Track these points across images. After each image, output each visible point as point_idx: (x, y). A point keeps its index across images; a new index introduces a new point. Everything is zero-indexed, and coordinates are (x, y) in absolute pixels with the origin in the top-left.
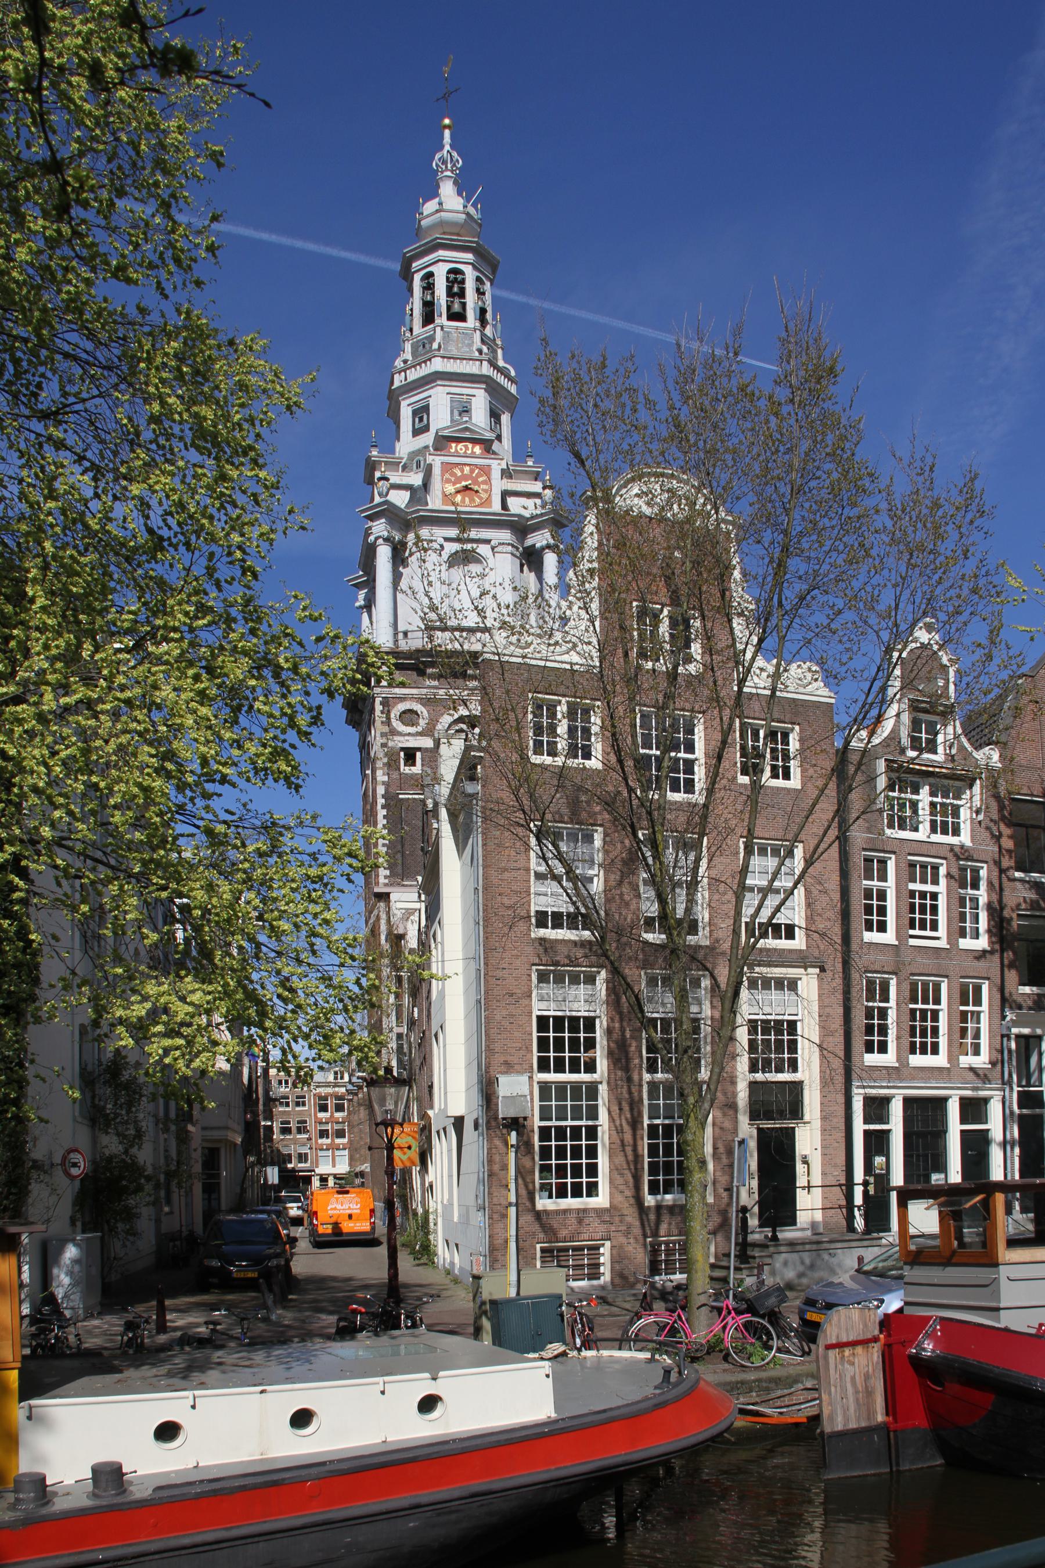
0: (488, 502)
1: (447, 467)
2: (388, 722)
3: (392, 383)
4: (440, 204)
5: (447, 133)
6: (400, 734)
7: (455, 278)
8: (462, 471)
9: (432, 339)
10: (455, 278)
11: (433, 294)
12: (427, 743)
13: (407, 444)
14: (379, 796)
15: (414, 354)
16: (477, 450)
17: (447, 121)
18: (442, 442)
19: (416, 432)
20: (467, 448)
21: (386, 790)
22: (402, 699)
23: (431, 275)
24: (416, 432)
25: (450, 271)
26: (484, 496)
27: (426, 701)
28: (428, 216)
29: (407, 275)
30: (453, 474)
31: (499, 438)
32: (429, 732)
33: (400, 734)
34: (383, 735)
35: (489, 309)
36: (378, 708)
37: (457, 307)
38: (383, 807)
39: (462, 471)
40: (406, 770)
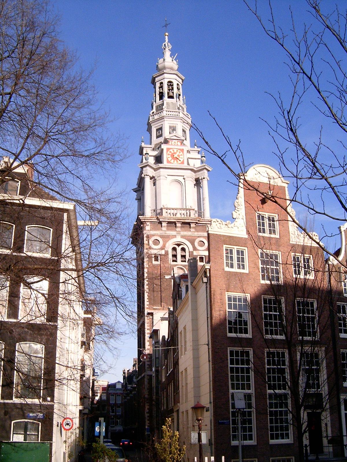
0: (183, 163)
1: (168, 149)
2: (148, 244)
3: (149, 120)
4: (164, 60)
5: (167, 37)
6: (153, 249)
7: (170, 84)
8: (174, 151)
9: (163, 104)
10: (170, 84)
11: (163, 90)
12: (163, 252)
13: (155, 141)
14: (145, 273)
15: (157, 110)
16: (179, 144)
17: (167, 34)
18: (166, 141)
19: (158, 137)
20: (175, 143)
21: (148, 271)
22: (153, 235)
23: (161, 83)
24: (158, 137)
25: (168, 82)
26: (182, 160)
27: (161, 237)
28: (160, 64)
29: (153, 82)
30: (170, 152)
31: (186, 139)
32: (162, 248)
33: (153, 249)
34: (147, 249)
35: (181, 95)
36: (145, 239)
37: (171, 94)
38: (147, 285)
39: (174, 151)
40: (154, 262)
